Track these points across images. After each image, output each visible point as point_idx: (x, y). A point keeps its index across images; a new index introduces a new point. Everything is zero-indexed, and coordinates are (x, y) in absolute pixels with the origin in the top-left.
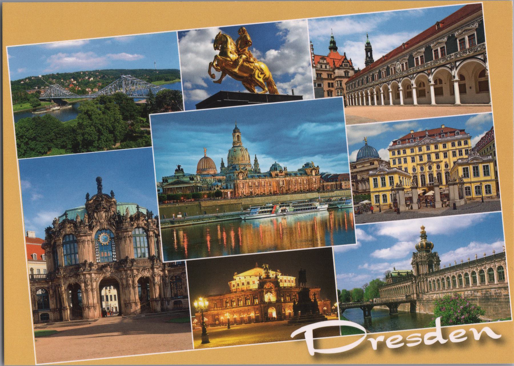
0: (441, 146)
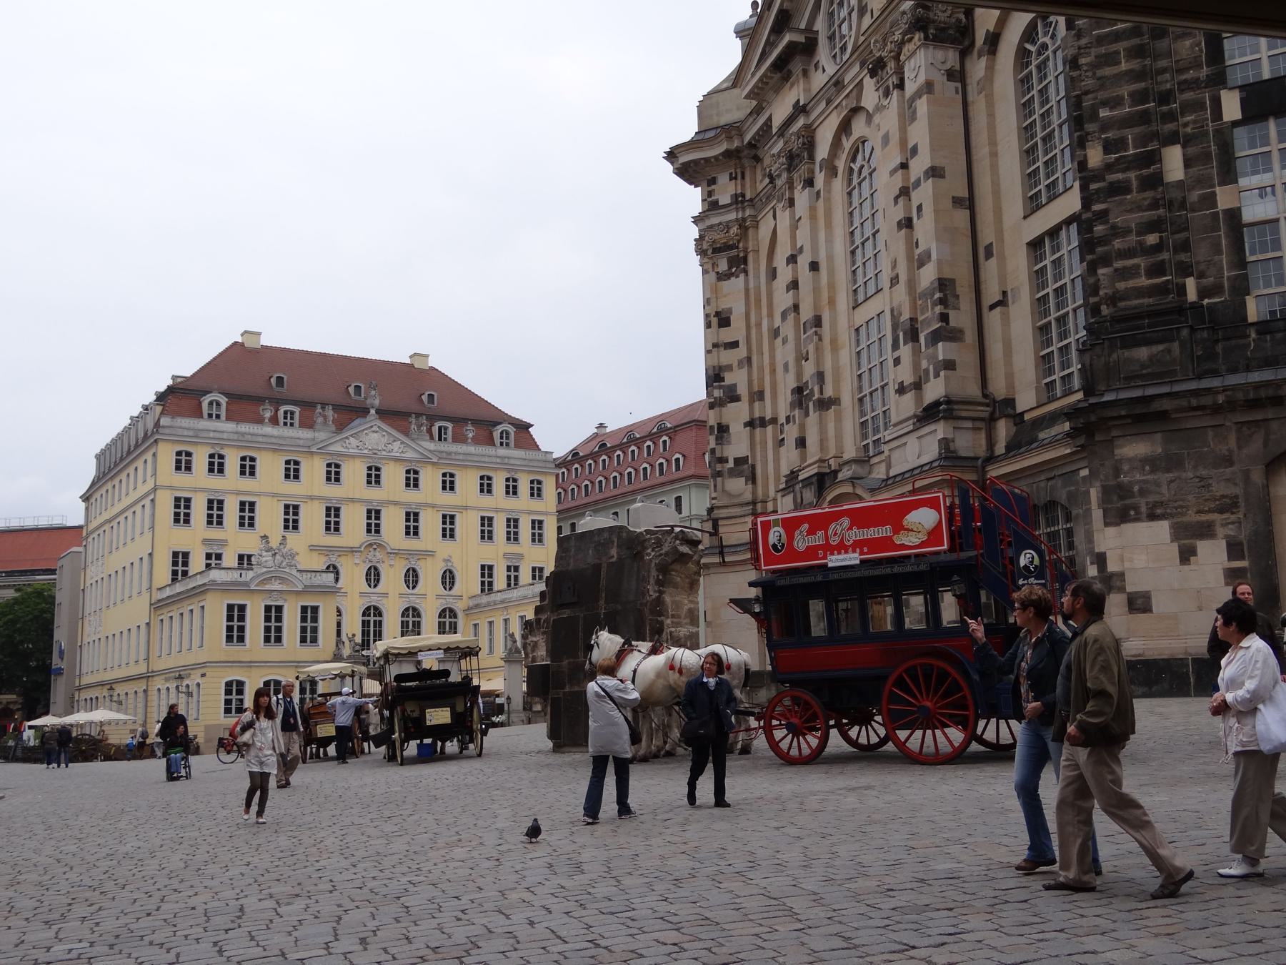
0: (430, 479)
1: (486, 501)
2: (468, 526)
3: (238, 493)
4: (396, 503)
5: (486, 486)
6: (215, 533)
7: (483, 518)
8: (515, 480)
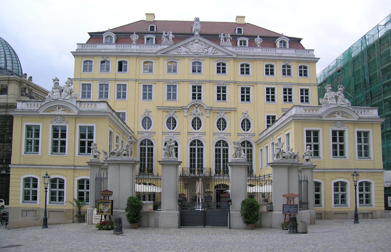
1: (270, 78)
4: (210, 82)
7: (268, 89)
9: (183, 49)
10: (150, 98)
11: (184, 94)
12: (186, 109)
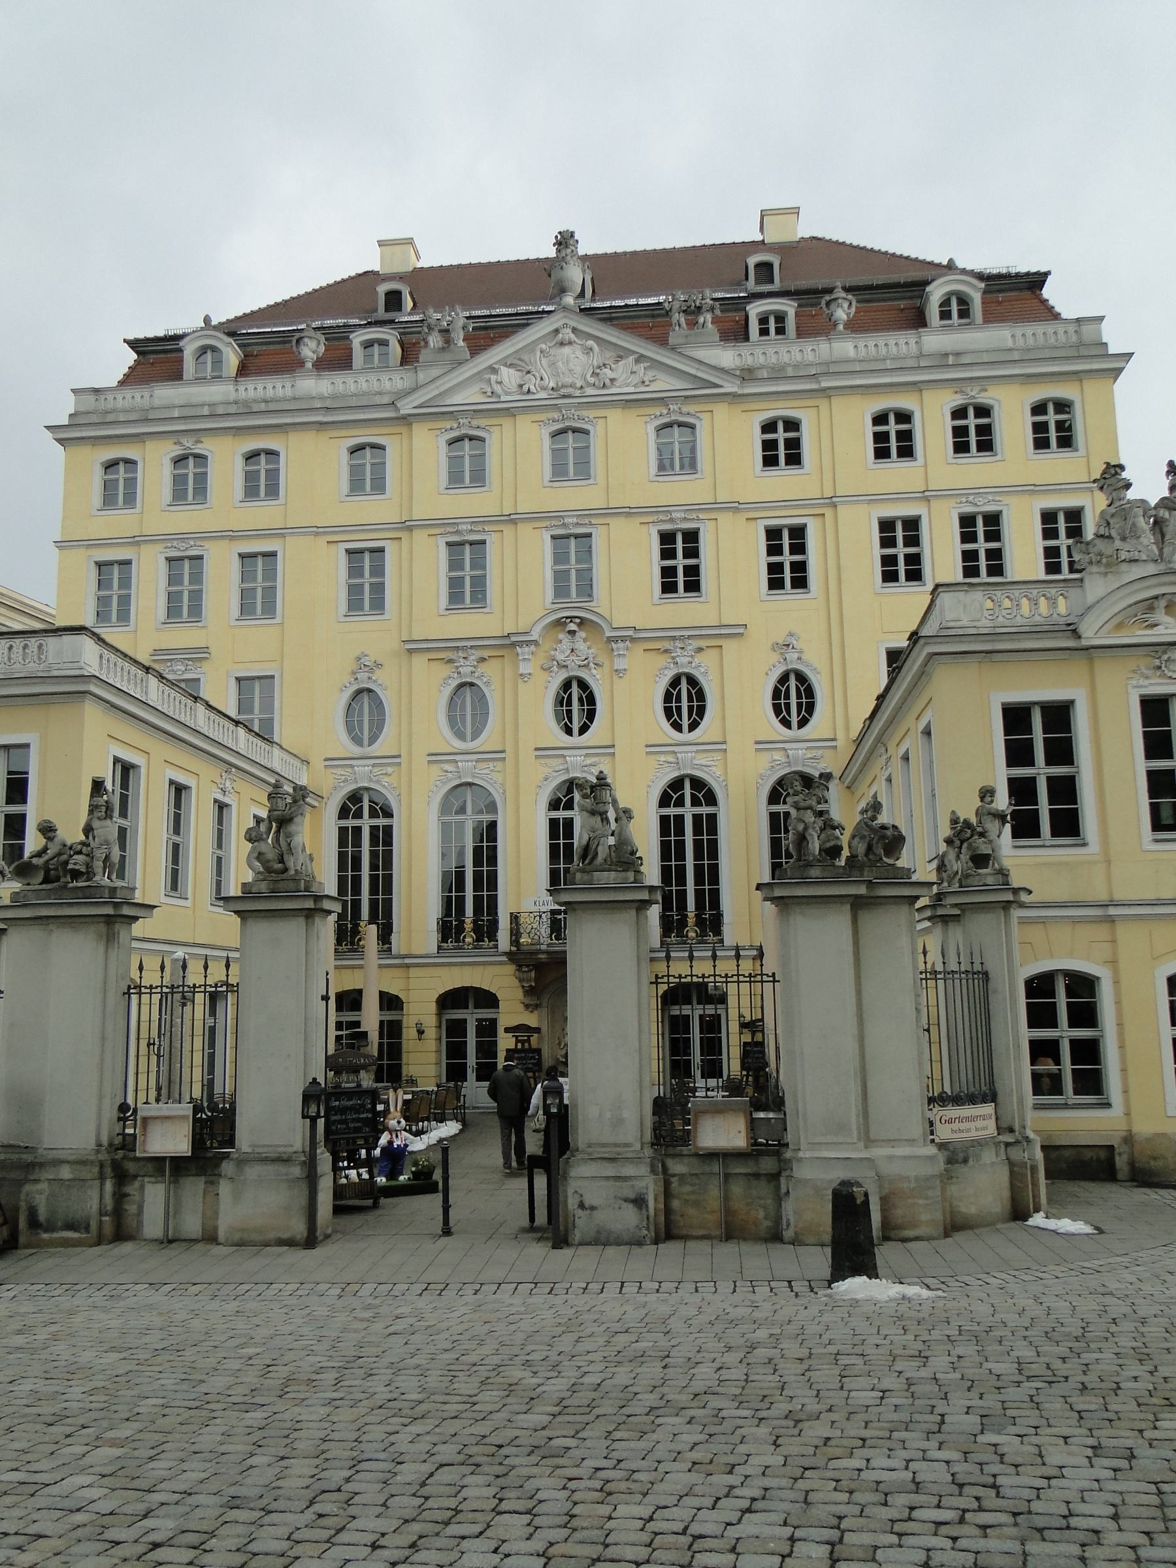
1: (897, 475)
2: (846, 550)
3: (232, 536)
4: (629, 513)
5: (894, 439)
6: (183, 637)
7: (886, 526)
8: (983, 411)
9: (509, 376)
10: (378, 604)
11: (523, 579)
12: (528, 643)
